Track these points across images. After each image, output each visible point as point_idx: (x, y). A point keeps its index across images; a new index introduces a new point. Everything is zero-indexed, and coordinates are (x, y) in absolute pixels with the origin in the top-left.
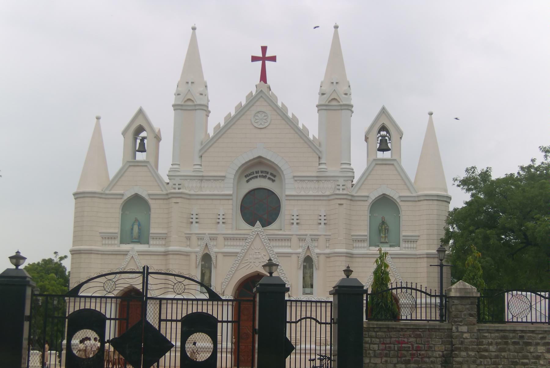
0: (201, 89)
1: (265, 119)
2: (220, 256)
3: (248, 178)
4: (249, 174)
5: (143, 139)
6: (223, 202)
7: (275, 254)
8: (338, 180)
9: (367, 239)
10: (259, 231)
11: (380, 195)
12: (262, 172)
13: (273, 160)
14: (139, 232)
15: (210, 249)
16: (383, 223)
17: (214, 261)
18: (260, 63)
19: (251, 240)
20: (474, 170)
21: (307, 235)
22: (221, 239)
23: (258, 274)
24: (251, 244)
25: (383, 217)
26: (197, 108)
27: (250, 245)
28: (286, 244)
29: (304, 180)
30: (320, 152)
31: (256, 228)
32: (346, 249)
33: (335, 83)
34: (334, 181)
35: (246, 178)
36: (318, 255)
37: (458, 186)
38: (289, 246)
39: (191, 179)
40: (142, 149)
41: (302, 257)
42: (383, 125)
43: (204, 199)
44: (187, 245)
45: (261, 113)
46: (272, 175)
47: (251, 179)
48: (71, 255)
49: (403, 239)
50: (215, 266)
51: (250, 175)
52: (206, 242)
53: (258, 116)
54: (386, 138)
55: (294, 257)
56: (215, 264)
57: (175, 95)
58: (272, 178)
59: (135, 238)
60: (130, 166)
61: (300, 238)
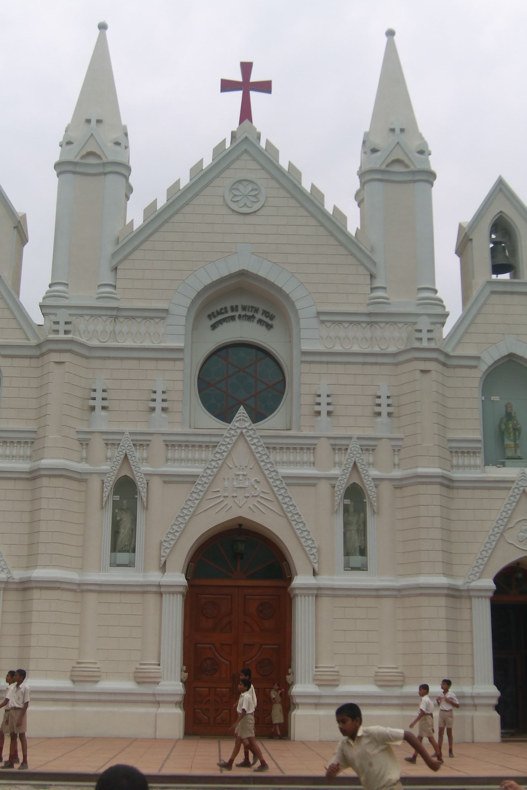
0: (117, 135)
1: (255, 196)
2: (156, 484)
3: (214, 321)
4: (217, 311)
6: (162, 365)
7: (282, 479)
8: (415, 323)
9: (480, 448)
10: (245, 428)
11: (503, 355)
12: (244, 308)
13: (271, 278)
15: (133, 467)
16: (509, 416)
17: (143, 494)
18: (239, 94)
21: (350, 438)
22: (158, 444)
23: (240, 525)
24: (228, 456)
25: (508, 403)
26: (109, 169)
27: (226, 459)
28: (305, 459)
29: (340, 322)
30: (374, 264)
31: (237, 421)
32: (440, 468)
33: (397, 131)
34: (406, 323)
35: (211, 319)
36: (377, 483)
38: (310, 463)
39: (92, 316)
41: (342, 486)
44: (82, 459)
45: (245, 183)
46: (267, 315)
47: (220, 322)
51: (219, 313)
53: (238, 189)
55: (324, 487)
56: (145, 499)
57: (61, 146)
58: (267, 320)
61: (336, 445)
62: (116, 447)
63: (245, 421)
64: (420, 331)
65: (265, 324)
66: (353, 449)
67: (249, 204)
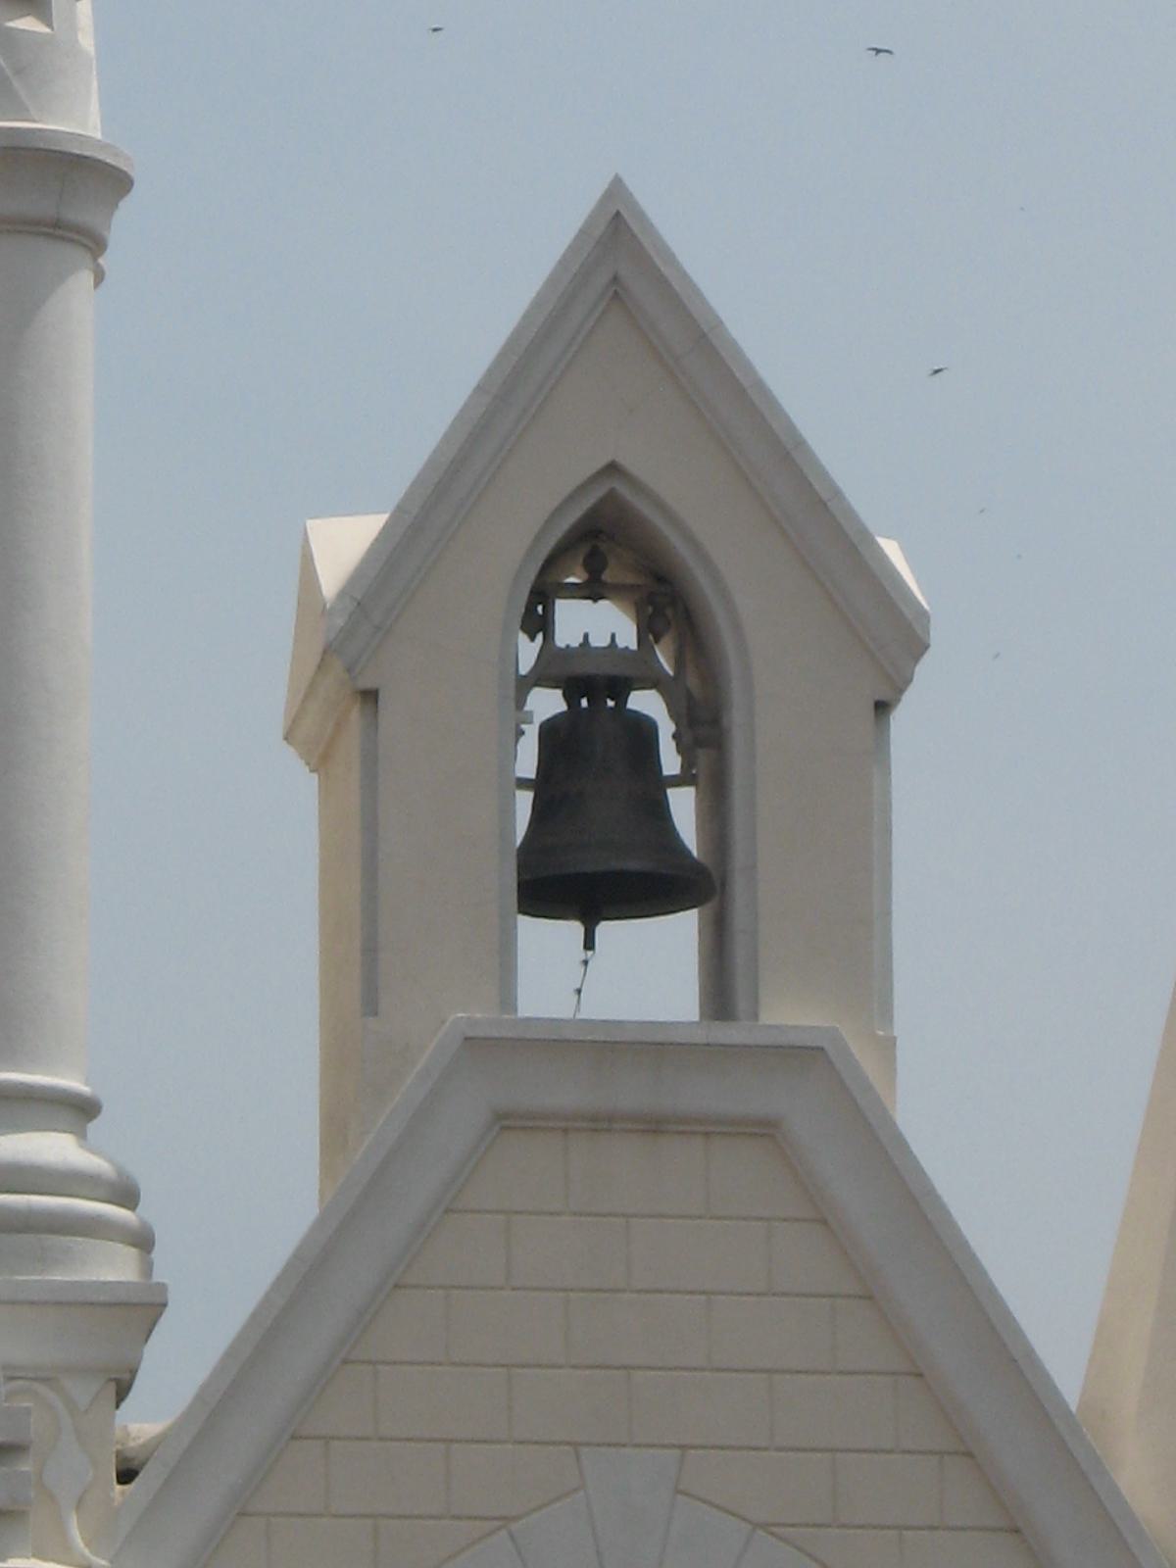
42: (612, 495)
54: (646, 702)
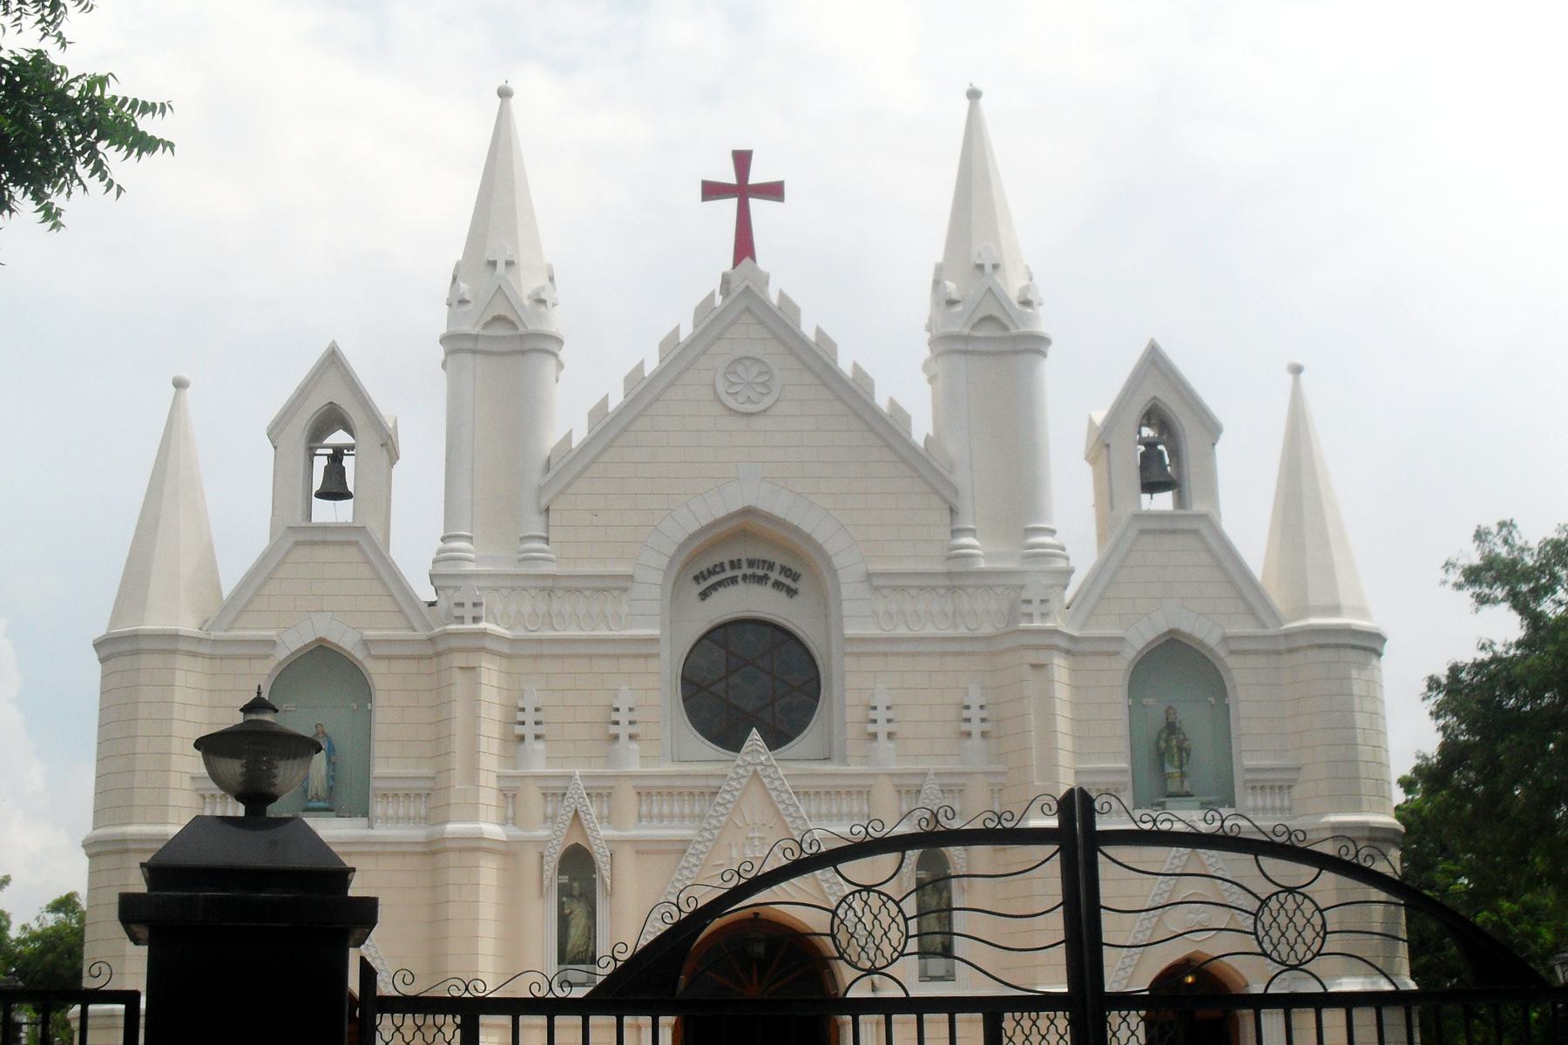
1: (764, 384)
3: (705, 585)
4: (708, 569)
5: (337, 456)
8: (1022, 587)
12: (751, 563)
14: (331, 774)
15: (588, 831)
16: (1171, 728)
18: (731, 204)
19: (734, 796)
20: (1510, 533)
21: (924, 774)
25: (1170, 707)
29: (903, 589)
30: (956, 492)
31: (748, 753)
35: (699, 583)
37: (1459, 586)
40: (335, 489)
43: (562, 657)
46: (788, 573)
47: (714, 587)
48: (87, 859)
49: (1246, 781)
50: (609, 888)
51: (711, 572)
52: (572, 806)
53: (736, 373)
54: (1161, 447)
56: (608, 881)
57: (449, 305)
58: (788, 581)
59: (317, 794)
60: (297, 543)
61: (902, 785)
62: (560, 798)
63: (760, 752)
64: (1029, 602)
65: (785, 589)
66: (928, 792)
67: (754, 397)
